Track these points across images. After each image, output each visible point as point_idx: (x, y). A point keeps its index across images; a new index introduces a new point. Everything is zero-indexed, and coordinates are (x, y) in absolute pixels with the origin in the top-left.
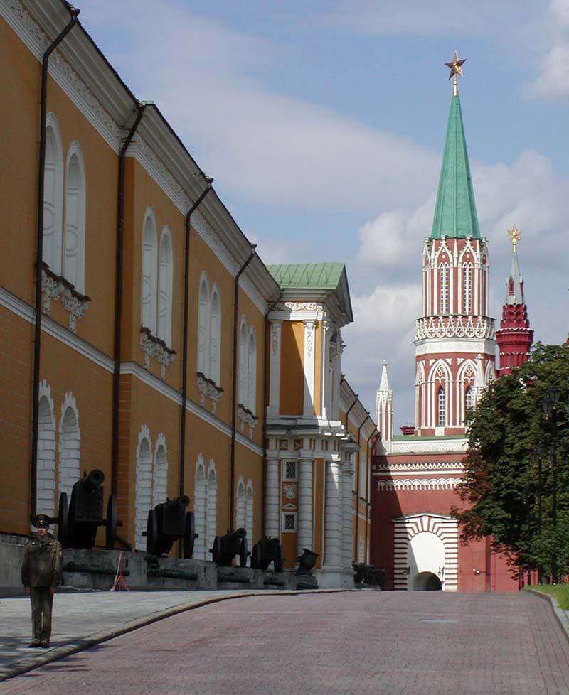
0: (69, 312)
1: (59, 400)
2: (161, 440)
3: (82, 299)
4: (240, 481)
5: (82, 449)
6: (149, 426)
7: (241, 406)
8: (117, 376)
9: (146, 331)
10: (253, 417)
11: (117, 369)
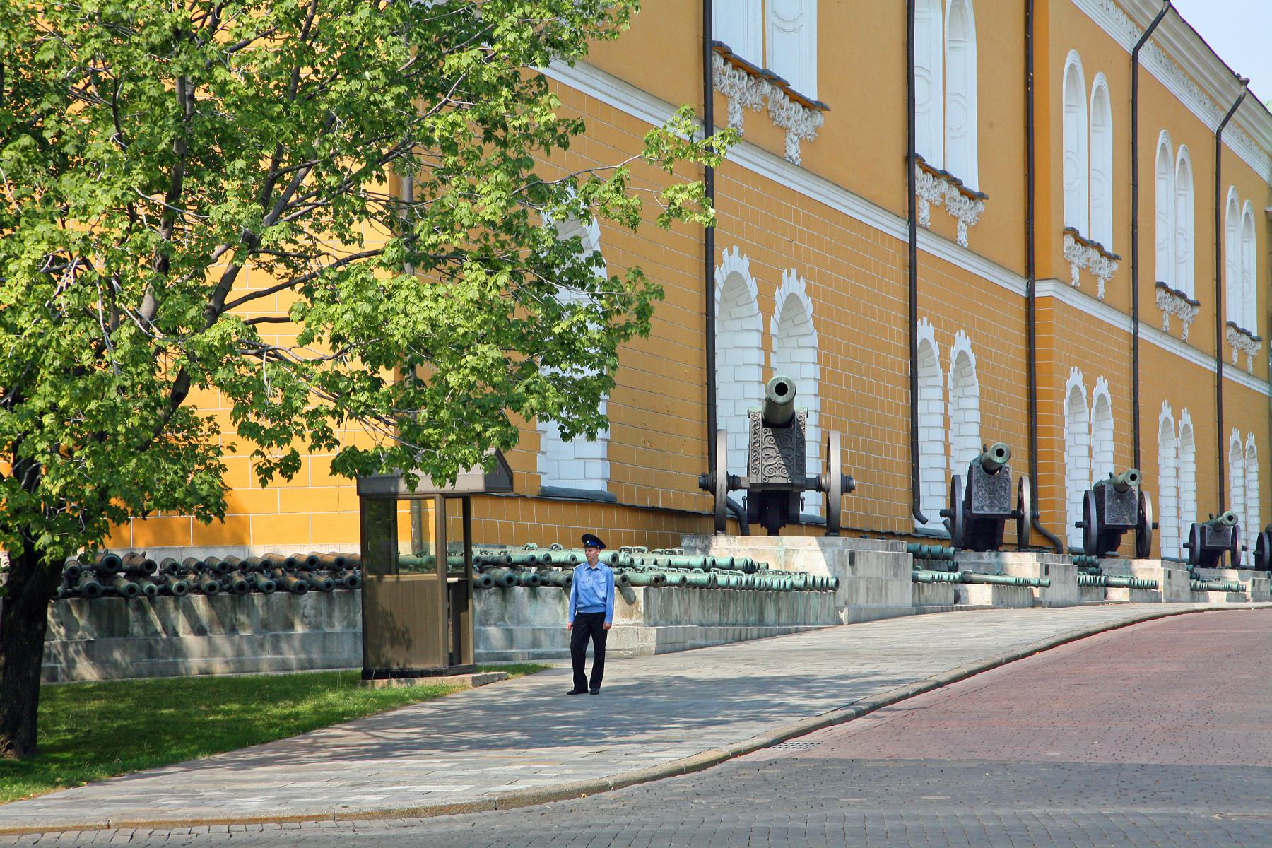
0: (956, 218)
1: (946, 341)
2: (1102, 387)
3: (973, 197)
4: (1234, 437)
5: (983, 407)
6: (1083, 368)
7: (1232, 325)
8: (1030, 301)
9: (1074, 232)
10: (1252, 339)
11: (1031, 290)
